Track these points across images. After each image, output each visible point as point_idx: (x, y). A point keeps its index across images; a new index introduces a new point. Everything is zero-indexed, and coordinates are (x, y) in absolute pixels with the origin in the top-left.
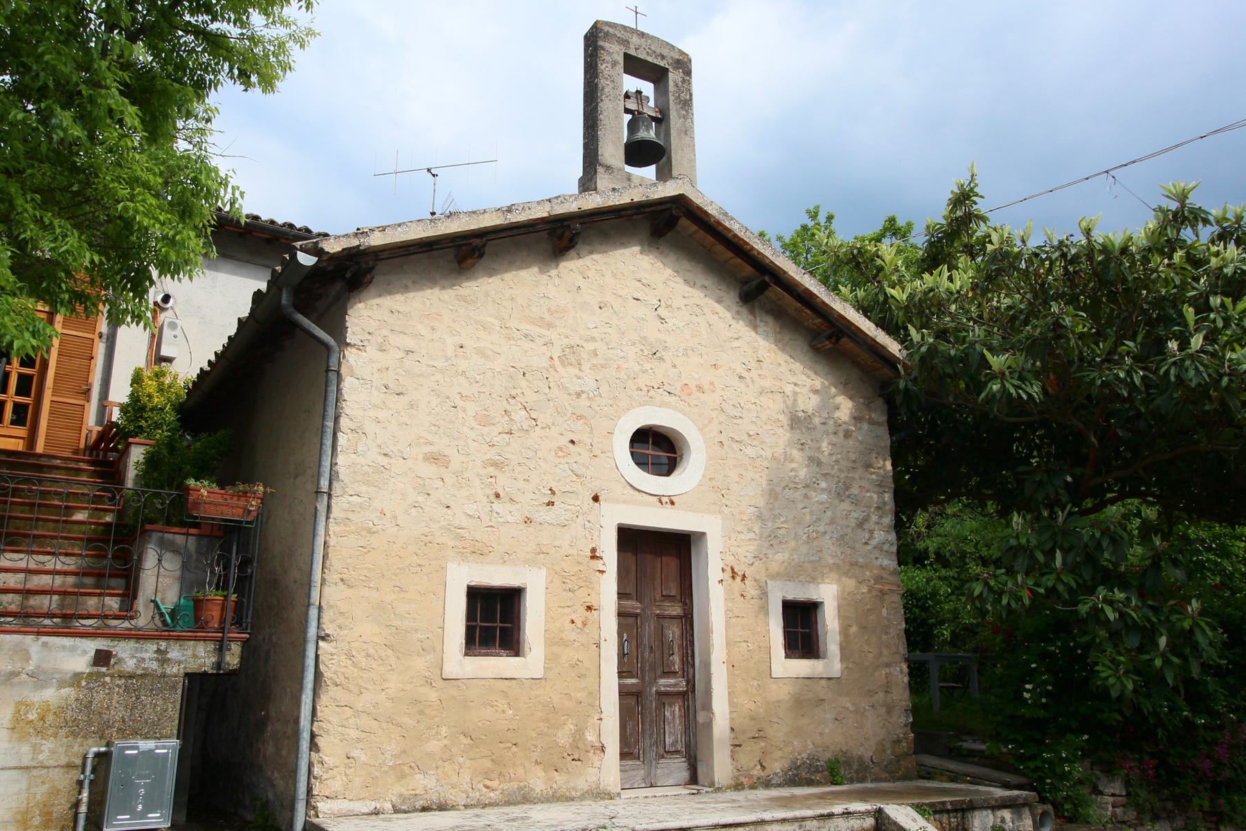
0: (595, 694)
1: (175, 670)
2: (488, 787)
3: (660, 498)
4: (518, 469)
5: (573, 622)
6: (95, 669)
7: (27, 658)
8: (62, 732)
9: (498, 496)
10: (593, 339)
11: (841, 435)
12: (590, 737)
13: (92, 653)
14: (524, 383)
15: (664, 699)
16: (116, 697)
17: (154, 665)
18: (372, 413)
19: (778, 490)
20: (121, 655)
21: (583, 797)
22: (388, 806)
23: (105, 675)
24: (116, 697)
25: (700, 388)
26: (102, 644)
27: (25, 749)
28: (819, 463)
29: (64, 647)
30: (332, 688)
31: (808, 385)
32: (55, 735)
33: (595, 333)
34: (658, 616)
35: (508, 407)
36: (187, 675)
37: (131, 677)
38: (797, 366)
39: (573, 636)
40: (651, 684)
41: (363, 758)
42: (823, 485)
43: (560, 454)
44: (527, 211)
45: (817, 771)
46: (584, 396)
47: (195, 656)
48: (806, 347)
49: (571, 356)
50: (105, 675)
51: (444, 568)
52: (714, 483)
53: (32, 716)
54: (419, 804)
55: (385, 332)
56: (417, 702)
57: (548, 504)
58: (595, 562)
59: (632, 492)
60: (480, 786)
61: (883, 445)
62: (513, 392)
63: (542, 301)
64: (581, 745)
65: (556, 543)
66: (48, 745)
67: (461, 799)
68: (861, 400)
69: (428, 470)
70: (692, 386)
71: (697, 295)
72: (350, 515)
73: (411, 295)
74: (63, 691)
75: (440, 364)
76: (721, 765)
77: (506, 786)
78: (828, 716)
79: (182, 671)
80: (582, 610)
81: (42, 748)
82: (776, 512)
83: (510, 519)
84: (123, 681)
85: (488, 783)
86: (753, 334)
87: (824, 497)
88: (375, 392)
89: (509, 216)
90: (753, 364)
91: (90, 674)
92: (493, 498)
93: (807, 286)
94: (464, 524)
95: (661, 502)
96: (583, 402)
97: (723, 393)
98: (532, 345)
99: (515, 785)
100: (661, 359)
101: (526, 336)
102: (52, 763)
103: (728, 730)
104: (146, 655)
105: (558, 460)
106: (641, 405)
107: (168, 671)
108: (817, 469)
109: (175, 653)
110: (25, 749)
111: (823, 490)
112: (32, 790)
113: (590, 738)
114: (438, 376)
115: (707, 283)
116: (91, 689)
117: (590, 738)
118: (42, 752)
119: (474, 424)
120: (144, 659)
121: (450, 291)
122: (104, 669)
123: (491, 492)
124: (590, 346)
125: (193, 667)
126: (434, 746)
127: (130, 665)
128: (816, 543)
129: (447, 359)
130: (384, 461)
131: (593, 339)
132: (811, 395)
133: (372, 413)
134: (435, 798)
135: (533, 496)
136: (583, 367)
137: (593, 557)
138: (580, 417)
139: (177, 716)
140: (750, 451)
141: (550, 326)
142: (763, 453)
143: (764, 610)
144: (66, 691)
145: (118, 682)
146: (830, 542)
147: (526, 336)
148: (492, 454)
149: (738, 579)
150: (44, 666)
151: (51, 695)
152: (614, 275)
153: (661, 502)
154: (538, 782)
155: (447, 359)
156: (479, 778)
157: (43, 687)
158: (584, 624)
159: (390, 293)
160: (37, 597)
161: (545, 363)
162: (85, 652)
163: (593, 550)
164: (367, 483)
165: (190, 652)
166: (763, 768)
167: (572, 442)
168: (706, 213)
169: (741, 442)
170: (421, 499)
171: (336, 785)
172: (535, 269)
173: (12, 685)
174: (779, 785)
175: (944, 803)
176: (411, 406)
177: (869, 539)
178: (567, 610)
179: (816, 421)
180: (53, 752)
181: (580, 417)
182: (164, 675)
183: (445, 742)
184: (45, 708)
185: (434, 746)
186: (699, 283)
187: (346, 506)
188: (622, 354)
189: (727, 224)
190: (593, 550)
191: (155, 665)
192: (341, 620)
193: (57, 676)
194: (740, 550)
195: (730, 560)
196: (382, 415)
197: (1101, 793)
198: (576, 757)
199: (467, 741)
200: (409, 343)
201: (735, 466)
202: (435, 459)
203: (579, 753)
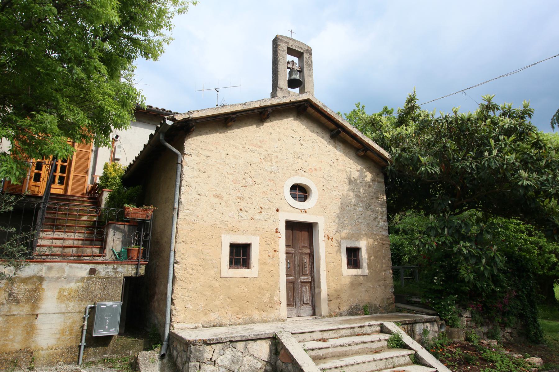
0: (277, 283)
1: (120, 276)
2: (238, 318)
5: (269, 256)
6: (90, 275)
7: (64, 272)
8: (77, 299)
9: (241, 210)
10: (276, 152)
12: (276, 298)
13: (89, 270)
14: (250, 168)
15: (303, 284)
16: (97, 286)
17: (112, 274)
19: (345, 207)
20: (99, 270)
21: (273, 321)
22: (200, 325)
24: (97, 286)
25: (316, 170)
27: (63, 306)
28: (359, 197)
29: (78, 267)
32: (75, 301)
33: (277, 149)
34: (301, 254)
35: (245, 177)
36: (124, 277)
37: (103, 278)
39: (269, 261)
41: (191, 307)
42: (361, 205)
43: (264, 194)
44: (252, 105)
45: (359, 310)
46: (273, 173)
47: (128, 270)
53: (66, 293)
54: (212, 325)
60: (235, 317)
62: (247, 172)
63: (257, 138)
66: (72, 304)
67: (228, 322)
69: (215, 200)
70: (313, 168)
72: (186, 217)
73: (209, 135)
74: (77, 284)
75: (219, 161)
76: (324, 308)
78: (363, 290)
79: (123, 276)
80: (273, 251)
81: (70, 305)
83: (245, 218)
84: (100, 280)
85: (238, 316)
90: (335, 161)
91: (88, 278)
92: (239, 211)
94: (228, 220)
96: (273, 175)
97: (324, 171)
98: (254, 154)
99: (248, 317)
100: (301, 159)
101: (251, 151)
102: (73, 311)
104: (109, 270)
105: (264, 196)
106: (294, 176)
107: (117, 276)
109: (120, 269)
110: (63, 306)
111: (361, 207)
112: (66, 321)
113: (275, 299)
114: (219, 166)
116: (88, 283)
117: (275, 299)
118: (69, 307)
119: (232, 183)
120: (108, 272)
121: (223, 134)
122: (93, 276)
123: (239, 208)
124: (275, 154)
125: (127, 274)
126: (218, 302)
127: (103, 274)
129: (222, 159)
130: (198, 197)
131: (276, 152)
134: (218, 322)
135: (254, 210)
136: (273, 162)
137: (276, 232)
138: (271, 181)
139: (121, 293)
140: (334, 193)
141: (260, 147)
142: (339, 193)
144: (78, 284)
145: (98, 280)
147: (251, 151)
148: (239, 194)
149: (330, 240)
150: (70, 275)
151: (73, 285)
152: (284, 128)
154: (256, 315)
156: (235, 314)
157: (70, 282)
158: (273, 257)
159: (201, 135)
160: (68, 249)
161: (259, 160)
162: (86, 269)
163: (277, 229)
165: (126, 269)
166: (340, 309)
170: (212, 211)
172: (255, 126)
173: (58, 282)
174: (345, 315)
175: (405, 321)
176: (209, 176)
178: (267, 252)
179: (358, 181)
180: (73, 307)
181: (271, 181)
182: (116, 278)
183: (222, 301)
184: (71, 290)
185: (218, 302)
187: (184, 214)
188: (287, 157)
189: (325, 109)
190: (277, 229)
191: (112, 274)
192: (182, 256)
193: (75, 278)
196: (198, 180)
197: (462, 317)
198: (270, 306)
199: (230, 301)
200: (208, 153)
202: (217, 196)
203: (271, 304)
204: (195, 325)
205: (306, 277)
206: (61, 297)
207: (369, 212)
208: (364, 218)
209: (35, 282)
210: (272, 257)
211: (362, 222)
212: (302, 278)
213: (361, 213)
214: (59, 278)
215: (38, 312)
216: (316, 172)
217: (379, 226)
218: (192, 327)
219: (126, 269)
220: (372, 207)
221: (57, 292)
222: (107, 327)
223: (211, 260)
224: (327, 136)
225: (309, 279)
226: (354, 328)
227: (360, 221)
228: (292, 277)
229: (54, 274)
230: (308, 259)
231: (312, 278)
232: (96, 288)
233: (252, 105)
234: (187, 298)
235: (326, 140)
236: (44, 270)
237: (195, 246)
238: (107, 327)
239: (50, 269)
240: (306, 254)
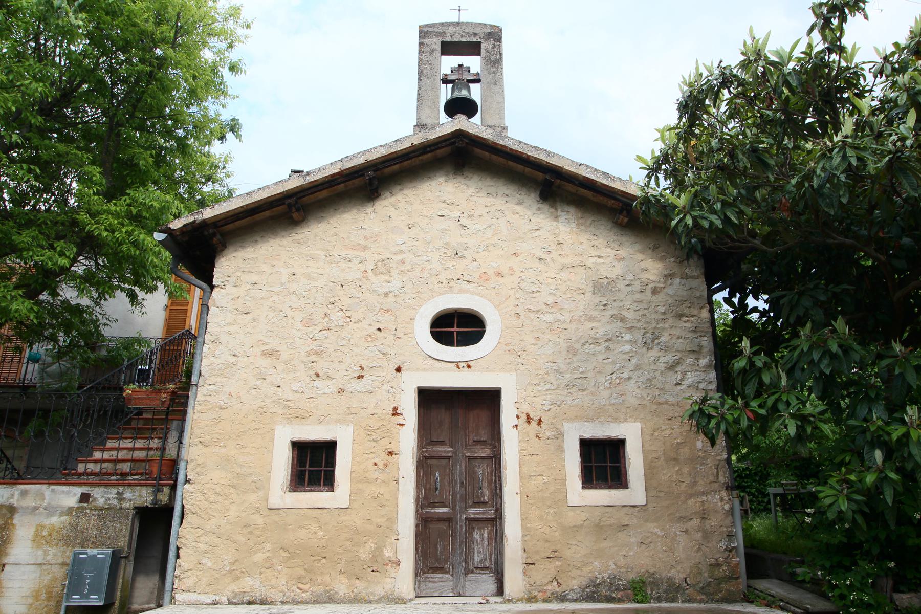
0: (392, 521)
1: (128, 505)
2: (301, 590)
4: (334, 354)
5: (375, 464)
6: (81, 505)
9: (317, 375)
10: (402, 252)
12: (388, 553)
13: (79, 495)
14: (341, 293)
16: (92, 522)
17: (115, 502)
18: (226, 329)
19: (578, 346)
20: (96, 496)
21: (379, 601)
23: (86, 508)
24: (92, 522)
25: (499, 274)
27: (40, 552)
28: (623, 319)
29: (63, 491)
32: (57, 545)
34: (470, 458)
35: (328, 311)
36: (136, 508)
37: (101, 509)
38: (600, 242)
39: (376, 475)
40: (461, 512)
41: (209, 564)
42: (627, 337)
43: (369, 339)
46: (391, 295)
47: (140, 496)
50: (86, 508)
52: (510, 347)
53: (45, 533)
54: (247, 598)
55: (239, 274)
56: (247, 525)
59: (432, 361)
60: (295, 588)
61: (698, 295)
62: (332, 301)
64: (379, 560)
65: (363, 406)
66: (52, 551)
67: (279, 597)
68: (672, 260)
69: (264, 362)
70: (491, 272)
71: (498, 203)
73: (259, 246)
74: (62, 518)
77: (315, 589)
79: (132, 505)
80: (384, 456)
81: (50, 552)
82: (575, 365)
83: (327, 391)
84: (97, 512)
85: (301, 586)
86: (554, 223)
87: (628, 348)
90: (553, 247)
91: (78, 508)
92: (314, 377)
93: (584, 174)
94: (290, 398)
96: (391, 298)
97: (522, 274)
98: (350, 264)
99: (322, 589)
100: (463, 257)
102: (54, 562)
103: (520, 552)
104: (111, 496)
105: (368, 344)
106: (441, 294)
107: (124, 506)
109: (128, 494)
110: (40, 552)
111: (627, 341)
112: (42, 578)
113: (387, 555)
114: (275, 297)
115: (507, 192)
116: (78, 517)
117: (387, 555)
118: (49, 555)
119: (300, 326)
120: (109, 498)
121: (288, 238)
122: (85, 505)
123: (312, 373)
124: (400, 257)
125: (139, 503)
126: (259, 557)
127: (101, 502)
128: (620, 388)
129: (282, 284)
130: (233, 359)
132: (616, 263)
133: (226, 329)
134: (258, 595)
135: (346, 373)
137: (393, 415)
138: (387, 311)
139: (128, 534)
140: (549, 318)
142: (560, 317)
143: (561, 449)
144: (64, 518)
145: (94, 513)
146: (635, 386)
148: (314, 346)
149: (534, 424)
150: (53, 503)
151: (56, 520)
154: (342, 587)
155: (282, 284)
156: (293, 582)
157: (51, 516)
158: (386, 466)
162: (75, 495)
163: (395, 409)
164: (221, 376)
165: (137, 494)
167: (379, 329)
168: (481, 138)
169: (538, 311)
170: (258, 383)
173: (35, 515)
176: (254, 320)
177: (682, 380)
178: (371, 456)
179: (621, 285)
180: (55, 555)
181: (387, 311)
182: (121, 509)
183: (268, 554)
185: (259, 557)
186: (501, 193)
187: (205, 392)
188: (428, 259)
190: (395, 409)
191: (115, 502)
192: (198, 470)
193: (59, 509)
195: (526, 408)
196: (232, 329)
198: (375, 569)
199: (285, 554)
200: (254, 278)
202: (270, 354)
204: (214, 597)
205: (481, 510)
206: (39, 539)
207: (654, 353)
208: (638, 367)
209: (4, 515)
210: (381, 466)
211: (629, 378)
212: (472, 510)
213: (627, 357)
214: (36, 508)
215: (5, 561)
216: (500, 279)
217: (687, 382)
219: (137, 494)
220: (664, 338)
221: (32, 531)
222: (86, 591)
223: (251, 475)
224: (531, 200)
225: (491, 512)
227: (625, 375)
228: (445, 510)
229: (30, 502)
230: (488, 471)
231: (496, 510)
232: (90, 525)
233: (323, 172)
234: (202, 547)
236: (16, 497)
237: (223, 450)
238: (86, 591)
239: (24, 494)
240: (483, 458)
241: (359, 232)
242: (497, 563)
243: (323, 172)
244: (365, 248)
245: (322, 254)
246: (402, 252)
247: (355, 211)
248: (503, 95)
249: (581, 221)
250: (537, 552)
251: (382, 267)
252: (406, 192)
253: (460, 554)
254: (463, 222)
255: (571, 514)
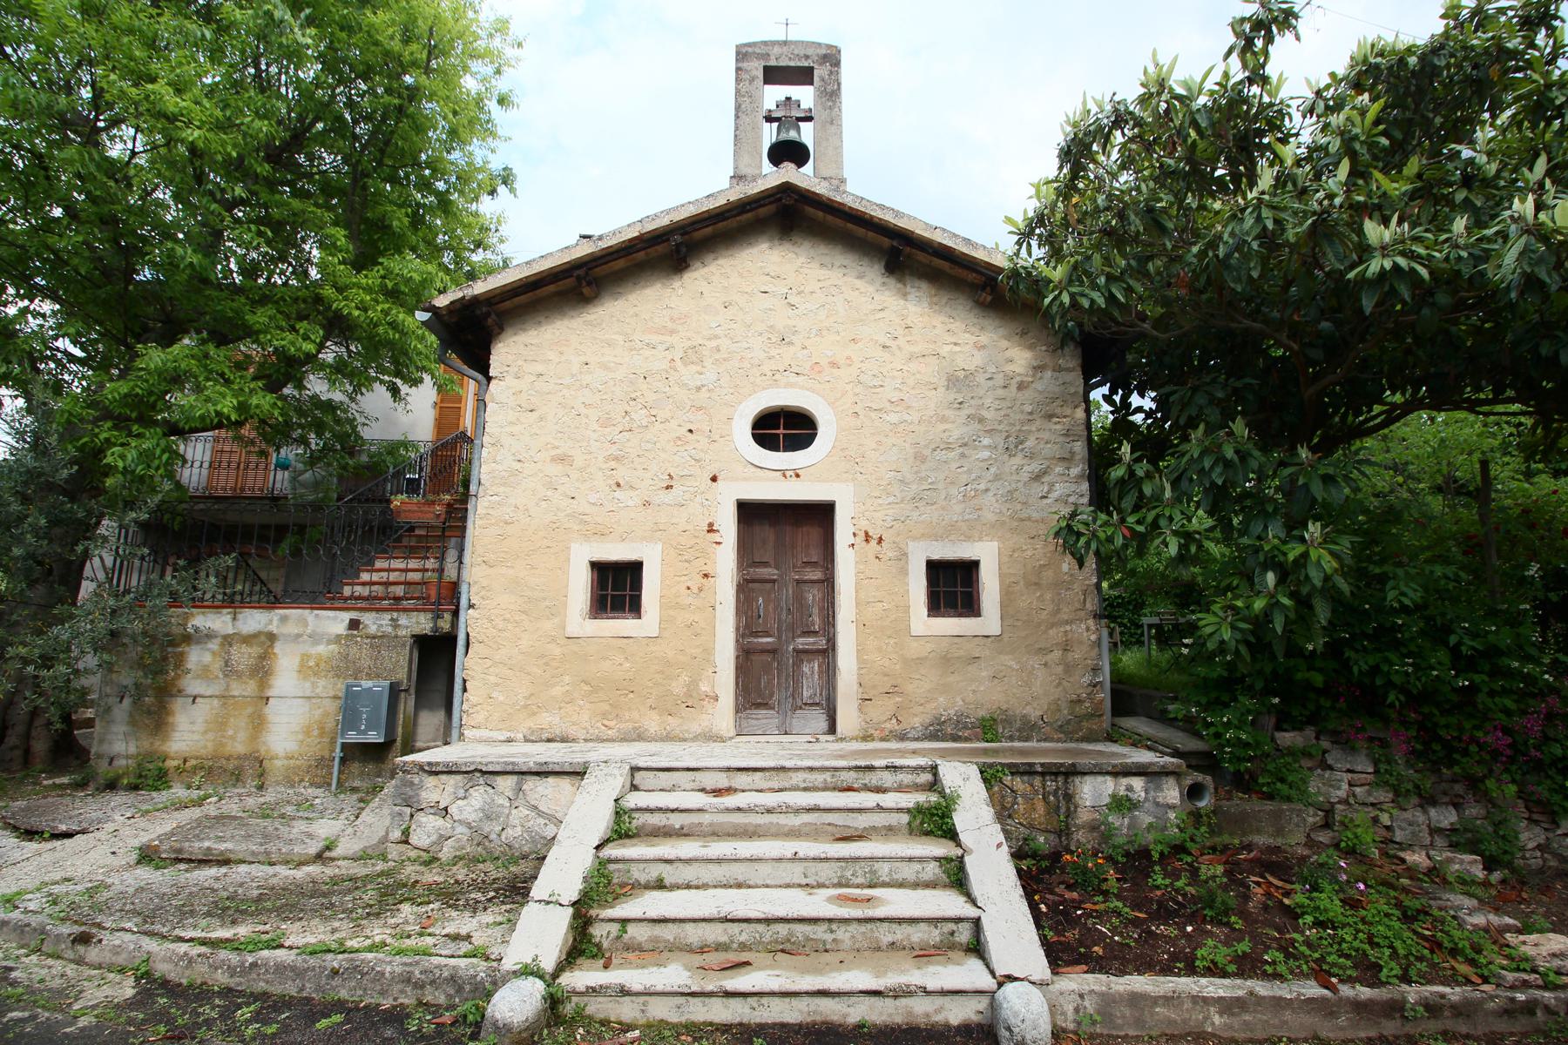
0: (708, 652)
3: (784, 473)
4: (637, 460)
7: (306, 625)
8: (330, 675)
9: (618, 485)
11: (1013, 388)
12: (704, 687)
17: (390, 629)
19: (927, 452)
20: (367, 622)
21: (695, 739)
22: (520, 736)
23: (356, 636)
25: (834, 365)
26: (354, 615)
28: (981, 420)
30: (476, 645)
31: (971, 342)
32: (326, 676)
34: (798, 582)
35: (628, 409)
36: (413, 636)
37: (374, 638)
38: (957, 326)
39: (690, 600)
40: (788, 643)
41: (501, 698)
42: (986, 441)
43: (679, 443)
46: (704, 389)
47: (418, 623)
48: (970, 304)
49: (692, 355)
50: (356, 636)
51: (569, 548)
52: (847, 453)
53: (311, 663)
54: (544, 737)
56: (543, 656)
57: (667, 488)
58: (712, 534)
59: (753, 469)
60: (599, 724)
61: (1072, 391)
62: (633, 396)
64: (694, 694)
65: (674, 521)
67: (581, 735)
68: (1044, 348)
69: (555, 470)
70: (824, 362)
72: (490, 511)
75: (567, 380)
77: (622, 726)
82: (923, 474)
83: (630, 503)
86: (902, 302)
87: (986, 454)
88: (511, 412)
89: (600, 243)
90: (900, 331)
92: (615, 487)
95: (785, 476)
96: (704, 394)
100: (791, 343)
104: (384, 622)
106: (764, 389)
108: (979, 426)
111: (985, 447)
115: (845, 262)
119: (596, 426)
123: (613, 482)
124: (714, 343)
125: (417, 631)
126: (557, 691)
127: (373, 629)
128: (975, 501)
129: (573, 376)
132: (975, 352)
135: (651, 482)
136: (705, 364)
138: (700, 408)
140: (893, 418)
142: (909, 418)
143: (904, 572)
144: (332, 647)
146: (994, 500)
148: (613, 450)
149: (873, 543)
150: (318, 630)
151: (322, 649)
153: (785, 476)
154: (652, 723)
155: (573, 376)
157: (318, 644)
158: (700, 590)
162: (342, 621)
163: (711, 525)
164: (504, 485)
165: (414, 620)
167: (691, 431)
169: (880, 410)
170: (549, 493)
171: (479, 718)
176: (541, 419)
178: (683, 578)
179: (981, 378)
181: (700, 408)
182: (396, 637)
183: (567, 688)
185: (557, 691)
186: (837, 263)
190: (711, 525)
191: (390, 629)
192: (483, 593)
194: (879, 515)
195: (864, 524)
196: (516, 429)
201: (873, 434)
202: (562, 459)
203: (693, 700)
204: (509, 734)
205: (811, 640)
206: (304, 670)
207: (1018, 460)
208: (997, 477)
210: (696, 591)
211: (987, 490)
212: (801, 640)
213: (985, 465)
214: (299, 636)
216: (835, 371)
218: (503, 738)
219: (414, 620)
221: (297, 660)
223: (545, 599)
224: (874, 271)
225: (822, 643)
226: (836, 769)
227: (982, 487)
228: (769, 640)
229: (291, 629)
230: (819, 596)
231: (828, 641)
232: (362, 654)
234: (492, 679)
235: (872, 282)
236: (275, 622)
237: (511, 571)
239: (284, 619)
240: (813, 582)
241: (665, 312)
242: (828, 699)
243: (618, 235)
244: (672, 332)
245: (620, 338)
246: (716, 337)
247: (658, 286)
248: (841, 137)
249: (935, 299)
250: (874, 687)
251: (692, 355)
252: (721, 261)
253: (787, 689)
254: (792, 299)
255: (915, 644)
